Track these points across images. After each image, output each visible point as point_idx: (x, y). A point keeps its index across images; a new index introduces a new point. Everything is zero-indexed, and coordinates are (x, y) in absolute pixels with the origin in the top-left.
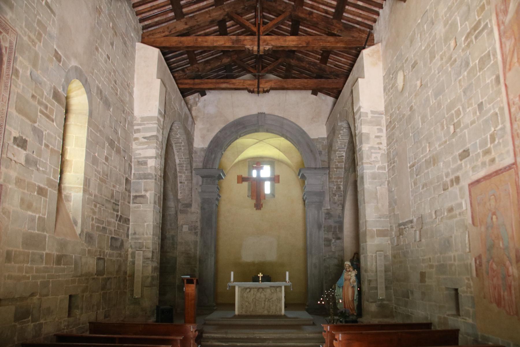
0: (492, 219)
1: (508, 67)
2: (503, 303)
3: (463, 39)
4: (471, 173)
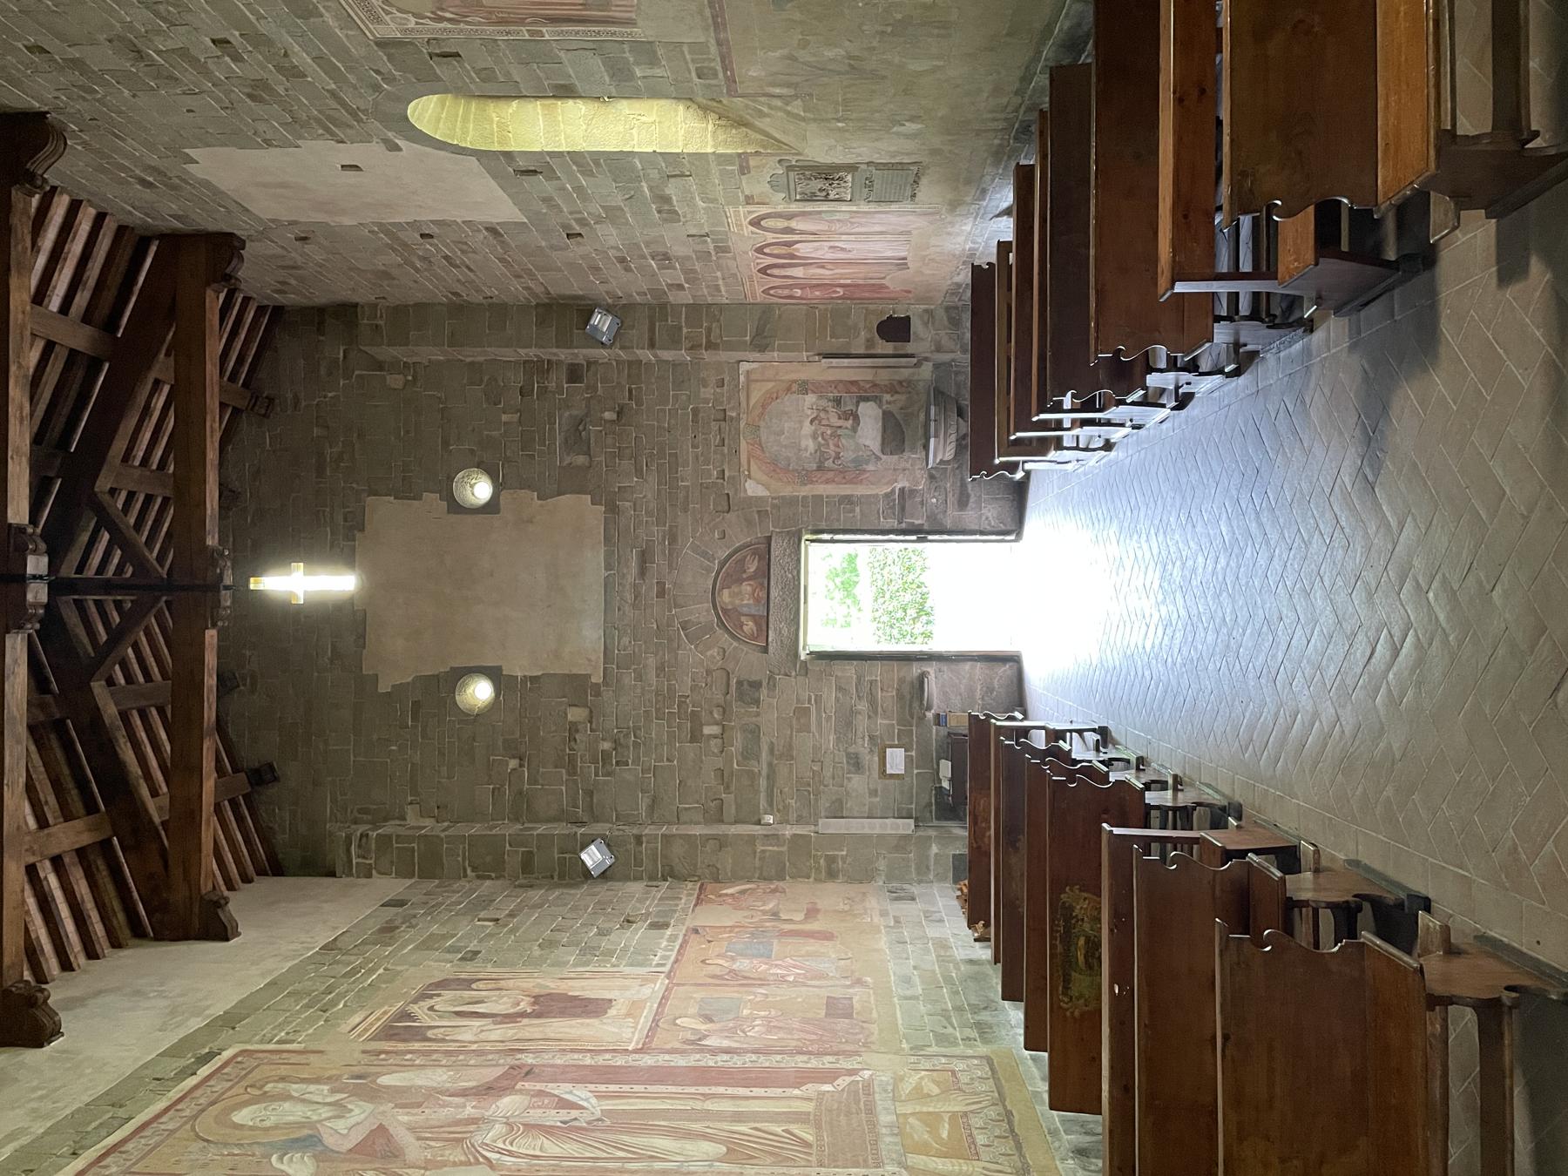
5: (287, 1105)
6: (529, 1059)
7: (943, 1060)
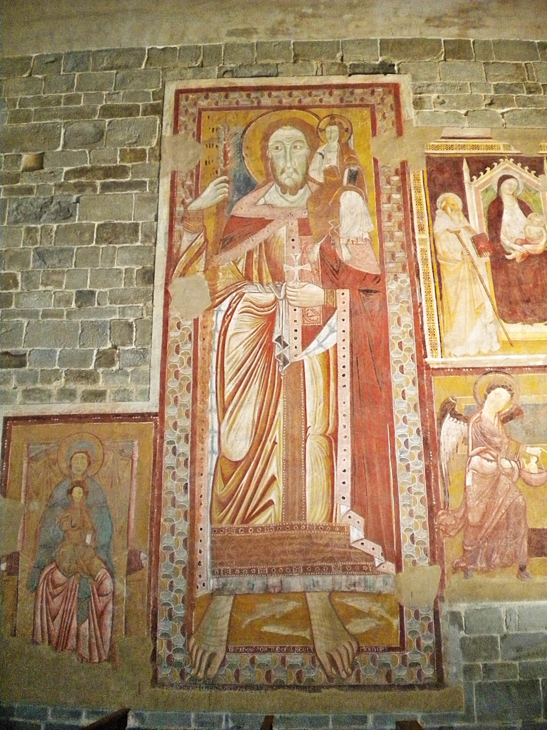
0: (70, 492)
1: (179, 268)
2: (72, 642)
3: (66, 169)
4: (19, 398)
5: (303, 151)
6: (396, 286)
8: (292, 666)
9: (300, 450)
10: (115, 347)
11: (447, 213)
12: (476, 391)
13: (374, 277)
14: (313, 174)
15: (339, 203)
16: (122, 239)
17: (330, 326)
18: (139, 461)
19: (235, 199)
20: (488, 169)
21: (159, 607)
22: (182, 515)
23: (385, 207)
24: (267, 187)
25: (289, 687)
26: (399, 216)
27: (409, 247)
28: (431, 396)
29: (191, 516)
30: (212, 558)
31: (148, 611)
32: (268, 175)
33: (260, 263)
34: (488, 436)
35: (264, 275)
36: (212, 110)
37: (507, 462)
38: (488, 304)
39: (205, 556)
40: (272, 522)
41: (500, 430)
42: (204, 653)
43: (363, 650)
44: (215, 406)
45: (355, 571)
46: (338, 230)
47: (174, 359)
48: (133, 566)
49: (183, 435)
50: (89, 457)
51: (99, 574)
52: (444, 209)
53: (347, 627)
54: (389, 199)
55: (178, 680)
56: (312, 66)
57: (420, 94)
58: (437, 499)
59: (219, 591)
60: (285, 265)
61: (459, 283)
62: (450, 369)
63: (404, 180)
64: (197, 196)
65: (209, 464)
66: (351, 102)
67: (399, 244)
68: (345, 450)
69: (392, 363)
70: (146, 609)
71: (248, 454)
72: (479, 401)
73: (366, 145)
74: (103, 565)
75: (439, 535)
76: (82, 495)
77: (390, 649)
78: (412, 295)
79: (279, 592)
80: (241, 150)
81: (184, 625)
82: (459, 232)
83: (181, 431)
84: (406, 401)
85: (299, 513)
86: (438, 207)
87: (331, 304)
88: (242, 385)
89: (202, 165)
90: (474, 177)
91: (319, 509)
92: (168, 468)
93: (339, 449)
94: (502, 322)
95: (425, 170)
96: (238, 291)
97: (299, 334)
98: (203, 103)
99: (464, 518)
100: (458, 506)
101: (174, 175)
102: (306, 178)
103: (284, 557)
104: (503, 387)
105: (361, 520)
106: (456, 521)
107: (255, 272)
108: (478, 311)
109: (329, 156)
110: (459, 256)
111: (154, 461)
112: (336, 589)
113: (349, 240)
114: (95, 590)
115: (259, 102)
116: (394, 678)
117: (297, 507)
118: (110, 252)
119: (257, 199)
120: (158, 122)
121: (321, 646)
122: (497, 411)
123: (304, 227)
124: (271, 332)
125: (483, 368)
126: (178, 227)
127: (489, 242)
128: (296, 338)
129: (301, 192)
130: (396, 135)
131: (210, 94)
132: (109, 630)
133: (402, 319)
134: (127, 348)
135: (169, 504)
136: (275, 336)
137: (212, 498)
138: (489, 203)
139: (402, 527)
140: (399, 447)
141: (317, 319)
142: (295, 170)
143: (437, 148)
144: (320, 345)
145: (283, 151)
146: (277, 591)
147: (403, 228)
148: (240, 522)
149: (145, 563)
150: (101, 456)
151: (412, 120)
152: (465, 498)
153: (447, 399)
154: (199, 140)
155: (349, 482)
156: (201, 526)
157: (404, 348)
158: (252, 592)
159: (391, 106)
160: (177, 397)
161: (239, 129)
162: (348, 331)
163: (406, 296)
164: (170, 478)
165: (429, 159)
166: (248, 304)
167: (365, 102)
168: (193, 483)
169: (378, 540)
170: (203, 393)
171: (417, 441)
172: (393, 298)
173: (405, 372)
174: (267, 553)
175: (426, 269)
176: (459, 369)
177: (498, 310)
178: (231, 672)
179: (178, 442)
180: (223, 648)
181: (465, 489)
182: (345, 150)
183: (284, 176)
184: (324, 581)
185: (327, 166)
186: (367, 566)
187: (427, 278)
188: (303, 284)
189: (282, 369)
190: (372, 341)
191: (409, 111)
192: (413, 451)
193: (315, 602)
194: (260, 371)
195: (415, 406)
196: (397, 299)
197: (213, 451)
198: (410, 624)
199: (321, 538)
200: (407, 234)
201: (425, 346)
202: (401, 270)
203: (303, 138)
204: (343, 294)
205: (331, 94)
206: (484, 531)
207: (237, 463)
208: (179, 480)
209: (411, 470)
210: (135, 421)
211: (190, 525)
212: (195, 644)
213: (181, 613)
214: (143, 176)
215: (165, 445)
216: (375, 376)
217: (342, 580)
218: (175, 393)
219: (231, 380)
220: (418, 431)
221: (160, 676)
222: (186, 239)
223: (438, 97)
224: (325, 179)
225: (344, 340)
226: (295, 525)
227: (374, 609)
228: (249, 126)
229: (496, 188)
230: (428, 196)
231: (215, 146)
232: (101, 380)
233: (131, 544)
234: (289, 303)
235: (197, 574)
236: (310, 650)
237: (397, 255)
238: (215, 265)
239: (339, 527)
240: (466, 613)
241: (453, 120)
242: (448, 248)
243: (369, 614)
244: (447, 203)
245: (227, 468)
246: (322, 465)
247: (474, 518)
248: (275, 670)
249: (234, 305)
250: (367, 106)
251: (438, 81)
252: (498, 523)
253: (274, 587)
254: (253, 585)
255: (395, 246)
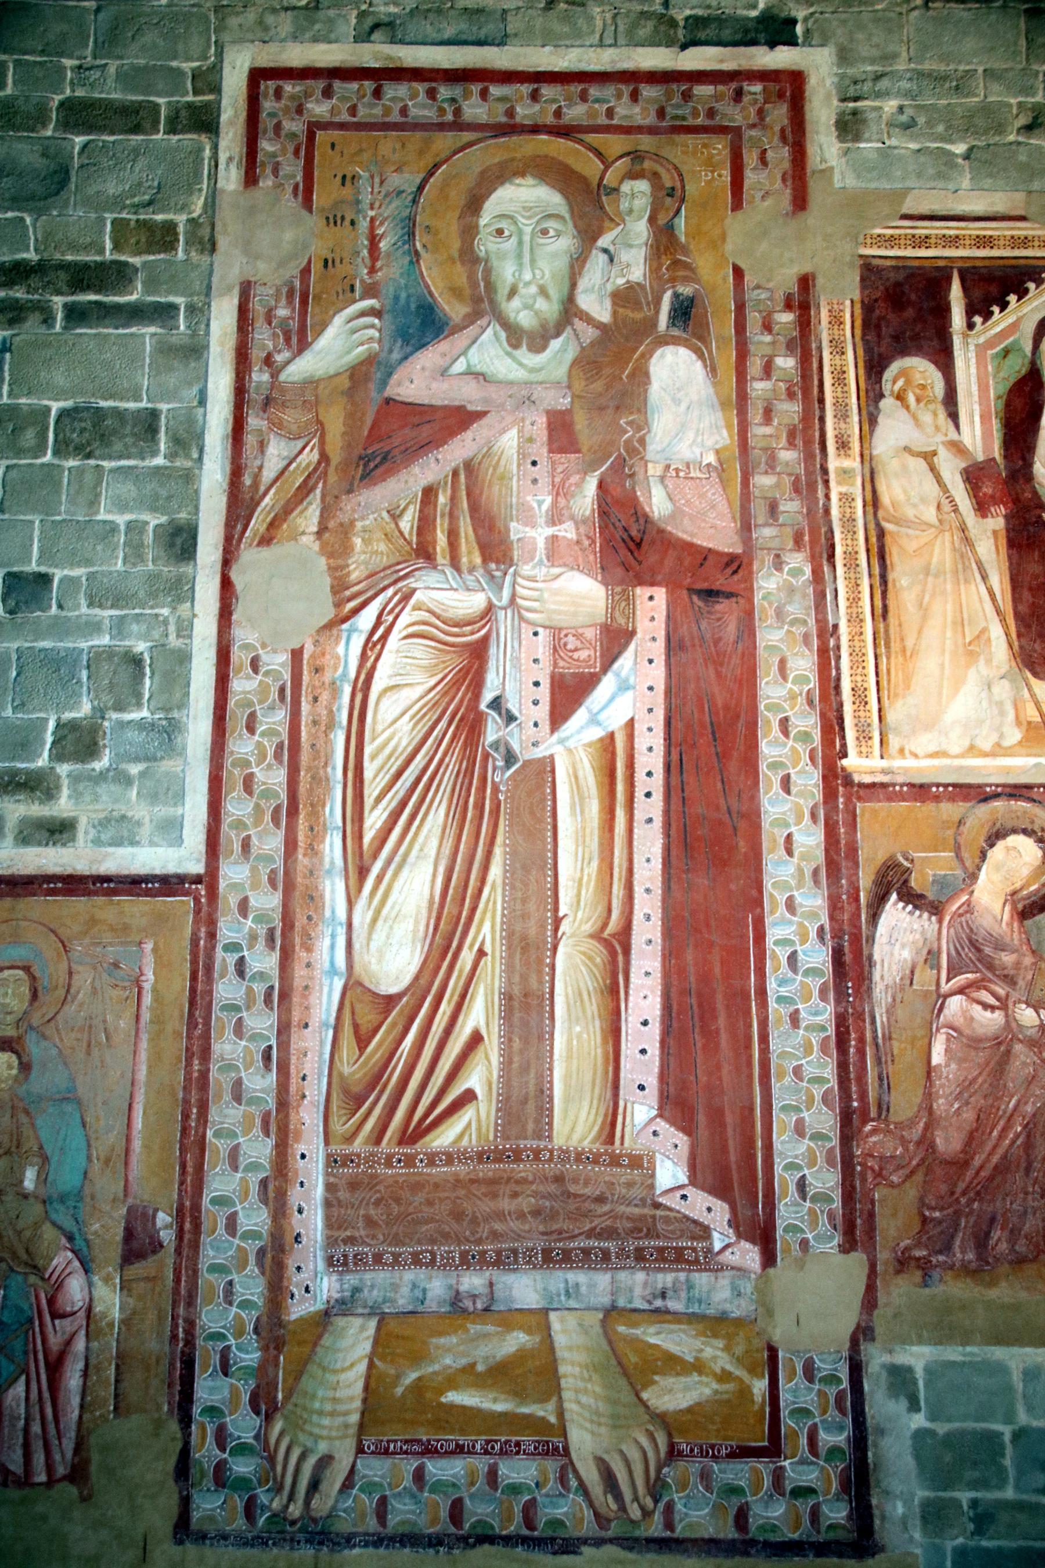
1: (258, 523)
5: (562, 244)
6: (778, 584)
7: (835, 1438)
8: (515, 1489)
9: (540, 972)
10: (100, 712)
11: (908, 408)
12: (962, 840)
13: (726, 559)
14: (586, 302)
15: (647, 375)
16: (118, 446)
17: (618, 675)
18: (155, 990)
19: (396, 356)
20: (1012, 298)
21: (199, 1342)
22: (258, 1121)
23: (759, 388)
24: (472, 330)
25: (508, 1541)
26: (790, 410)
27: (812, 487)
28: (853, 851)
29: (280, 1124)
30: (330, 1223)
31: (173, 1353)
32: (477, 300)
33: (452, 516)
34: (987, 950)
35: (463, 548)
36: (342, 126)
37: (1030, 1012)
38: (996, 632)
39: (312, 1223)
40: (472, 1142)
41: (1016, 936)
42: (303, 1457)
43: (680, 1454)
44: (339, 862)
45: (665, 1260)
46: (642, 441)
47: (241, 746)
48: (137, 1245)
49: (262, 931)
50: (33, 978)
51: (55, 1262)
52: (900, 397)
53: (645, 1395)
54: (768, 369)
55: (240, 1523)
56: (590, 19)
57: (856, 99)
58: (863, 1096)
59: (342, 1307)
60: (513, 525)
61: (930, 579)
62: (902, 785)
63: (805, 324)
64: (303, 345)
65: (325, 1000)
66: (684, 118)
67: (787, 480)
68: (647, 974)
69: (763, 767)
70: (167, 1349)
71: (417, 978)
72: (968, 864)
73: (717, 231)
74: (64, 1241)
75: (864, 1180)
76: (14, 1072)
77: (743, 1452)
78: (817, 608)
79: (486, 1310)
80: (411, 235)
81: (258, 1386)
82: (934, 453)
83: (258, 920)
84: (795, 860)
85: (537, 1121)
86: (887, 393)
87: (622, 621)
88: (405, 813)
89: (316, 268)
90: (978, 319)
91: (583, 1114)
92: (224, 1008)
93: (633, 970)
94: (1029, 675)
95: (857, 297)
96: (400, 585)
97: (544, 693)
98: (319, 109)
99: (926, 1142)
100: (910, 1114)
101: (246, 290)
102: (569, 311)
103: (498, 1226)
104: (1025, 832)
105: (682, 1140)
106: (906, 1149)
107: (441, 539)
108: (972, 649)
109: (624, 256)
110: (930, 514)
111: (193, 990)
112: (621, 1303)
113: (668, 467)
114: (44, 1302)
115: (457, 112)
116: (753, 1524)
117: (531, 1106)
118: (89, 478)
119: (448, 360)
120: (207, 153)
121: (583, 1441)
122: (1009, 890)
123: (561, 433)
124: (477, 685)
125: (980, 786)
126: (254, 422)
127: (1005, 482)
128: (536, 703)
129: (555, 344)
130: (790, 208)
131: (337, 84)
132: (76, 1401)
133: (790, 664)
134: (128, 717)
135: (227, 1097)
136: (488, 696)
137: (329, 1084)
138: (1009, 385)
139: (777, 1160)
140: (777, 969)
141: (587, 656)
142: (543, 291)
143: (891, 241)
144: (594, 720)
145: (514, 240)
146: (479, 1306)
147: (799, 442)
148: (395, 1140)
149: (167, 1236)
150: (63, 977)
151: (832, 168)
152: (929, 1096)
153: (892, 857)
154: (308, 203)
155: (654, 1051)
156: (301, 1148)
157: (793, 733)
158: (420, 1309)
159: (783, 131)
160: (249, 837)
161: (407, 180)
162: (660, 687)
163: (801, 608)
164: (229, 1033)
165: (869, 270)
166: (424, 615)
167: (718, 120)
168: (284, 1045)
169: (721, 1189)
170: (312, 829)
171: (817, 956)
172: (771, 612)
173: (794, 790)
174: (458, 1215)
175: (850, 542)
176: (922, 786)
177: (1021, 647)
178: (369, 1503)
179: (251, 947)
180: (350, 1444)
181: (929, 1073)
182: (665, 243)
183: (516, 303)
184: (592, 1286)
185: (621, 281)
186: (694, 1250)
187: (851, 564)
188: (556, 571)
189: (500, 776)
190: (717, 714)
191: (825, 147)
192: (808, 980)
193: (569, 1335)
194: (447, 780)
195: (816, 873)
196: (779, 614)
197: (333, 971)
198: (795, 1391)
199: (586, 1183)
200: (809, 457)
201: (842, 729)
202: (790, 544)
203: (564, 210)
204: (651, 598)
205: (635, 96)
206: (970, 1174)
207: (391, 1000)
208: (253, 1038)
209: (803, 1025)
210: (148, 893)
211: (277, 1146)
212: (282, 1434)
213: (249, 1356)
214: (169, 292)
215: (219, 953)
216: (722, 802)
217: (637, 1284)
218: (245, 827)
219: (379, 799)
220: (821, 930)
221: (196, 1515)
222: (276, 454)
223: (901, 109)
224: (615, 313)
225: (650, 710)
226: (526, 1149)
227: (708, 1352)
228: (431, 174)
229: (1028, 348)
230: (861, 364)
231: (347, 222)
232: (65, 792)
233: (134, 1187)
234: (521, 618)
235: (291, 1263)
236: (556, 1449)
237: (782, 508)
238: (343, 517)
239: (630, 1156)
240: (927, 1370)
241: (931, 171)
242: (905, 491)
243: (698, 1367)
244: (908, 382)
245: (367, 1010)
246: (593, 1007)
247: (948, 1142)
248: (472, 1496)
249: (391, 618)
250: (723, 130)
251: (901, 66)
252: (1004, 1157)
253: (474, 1297)
254: (424, 1291)
255: (778, 485)
